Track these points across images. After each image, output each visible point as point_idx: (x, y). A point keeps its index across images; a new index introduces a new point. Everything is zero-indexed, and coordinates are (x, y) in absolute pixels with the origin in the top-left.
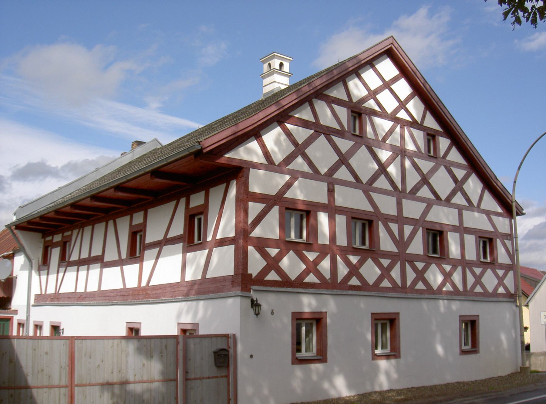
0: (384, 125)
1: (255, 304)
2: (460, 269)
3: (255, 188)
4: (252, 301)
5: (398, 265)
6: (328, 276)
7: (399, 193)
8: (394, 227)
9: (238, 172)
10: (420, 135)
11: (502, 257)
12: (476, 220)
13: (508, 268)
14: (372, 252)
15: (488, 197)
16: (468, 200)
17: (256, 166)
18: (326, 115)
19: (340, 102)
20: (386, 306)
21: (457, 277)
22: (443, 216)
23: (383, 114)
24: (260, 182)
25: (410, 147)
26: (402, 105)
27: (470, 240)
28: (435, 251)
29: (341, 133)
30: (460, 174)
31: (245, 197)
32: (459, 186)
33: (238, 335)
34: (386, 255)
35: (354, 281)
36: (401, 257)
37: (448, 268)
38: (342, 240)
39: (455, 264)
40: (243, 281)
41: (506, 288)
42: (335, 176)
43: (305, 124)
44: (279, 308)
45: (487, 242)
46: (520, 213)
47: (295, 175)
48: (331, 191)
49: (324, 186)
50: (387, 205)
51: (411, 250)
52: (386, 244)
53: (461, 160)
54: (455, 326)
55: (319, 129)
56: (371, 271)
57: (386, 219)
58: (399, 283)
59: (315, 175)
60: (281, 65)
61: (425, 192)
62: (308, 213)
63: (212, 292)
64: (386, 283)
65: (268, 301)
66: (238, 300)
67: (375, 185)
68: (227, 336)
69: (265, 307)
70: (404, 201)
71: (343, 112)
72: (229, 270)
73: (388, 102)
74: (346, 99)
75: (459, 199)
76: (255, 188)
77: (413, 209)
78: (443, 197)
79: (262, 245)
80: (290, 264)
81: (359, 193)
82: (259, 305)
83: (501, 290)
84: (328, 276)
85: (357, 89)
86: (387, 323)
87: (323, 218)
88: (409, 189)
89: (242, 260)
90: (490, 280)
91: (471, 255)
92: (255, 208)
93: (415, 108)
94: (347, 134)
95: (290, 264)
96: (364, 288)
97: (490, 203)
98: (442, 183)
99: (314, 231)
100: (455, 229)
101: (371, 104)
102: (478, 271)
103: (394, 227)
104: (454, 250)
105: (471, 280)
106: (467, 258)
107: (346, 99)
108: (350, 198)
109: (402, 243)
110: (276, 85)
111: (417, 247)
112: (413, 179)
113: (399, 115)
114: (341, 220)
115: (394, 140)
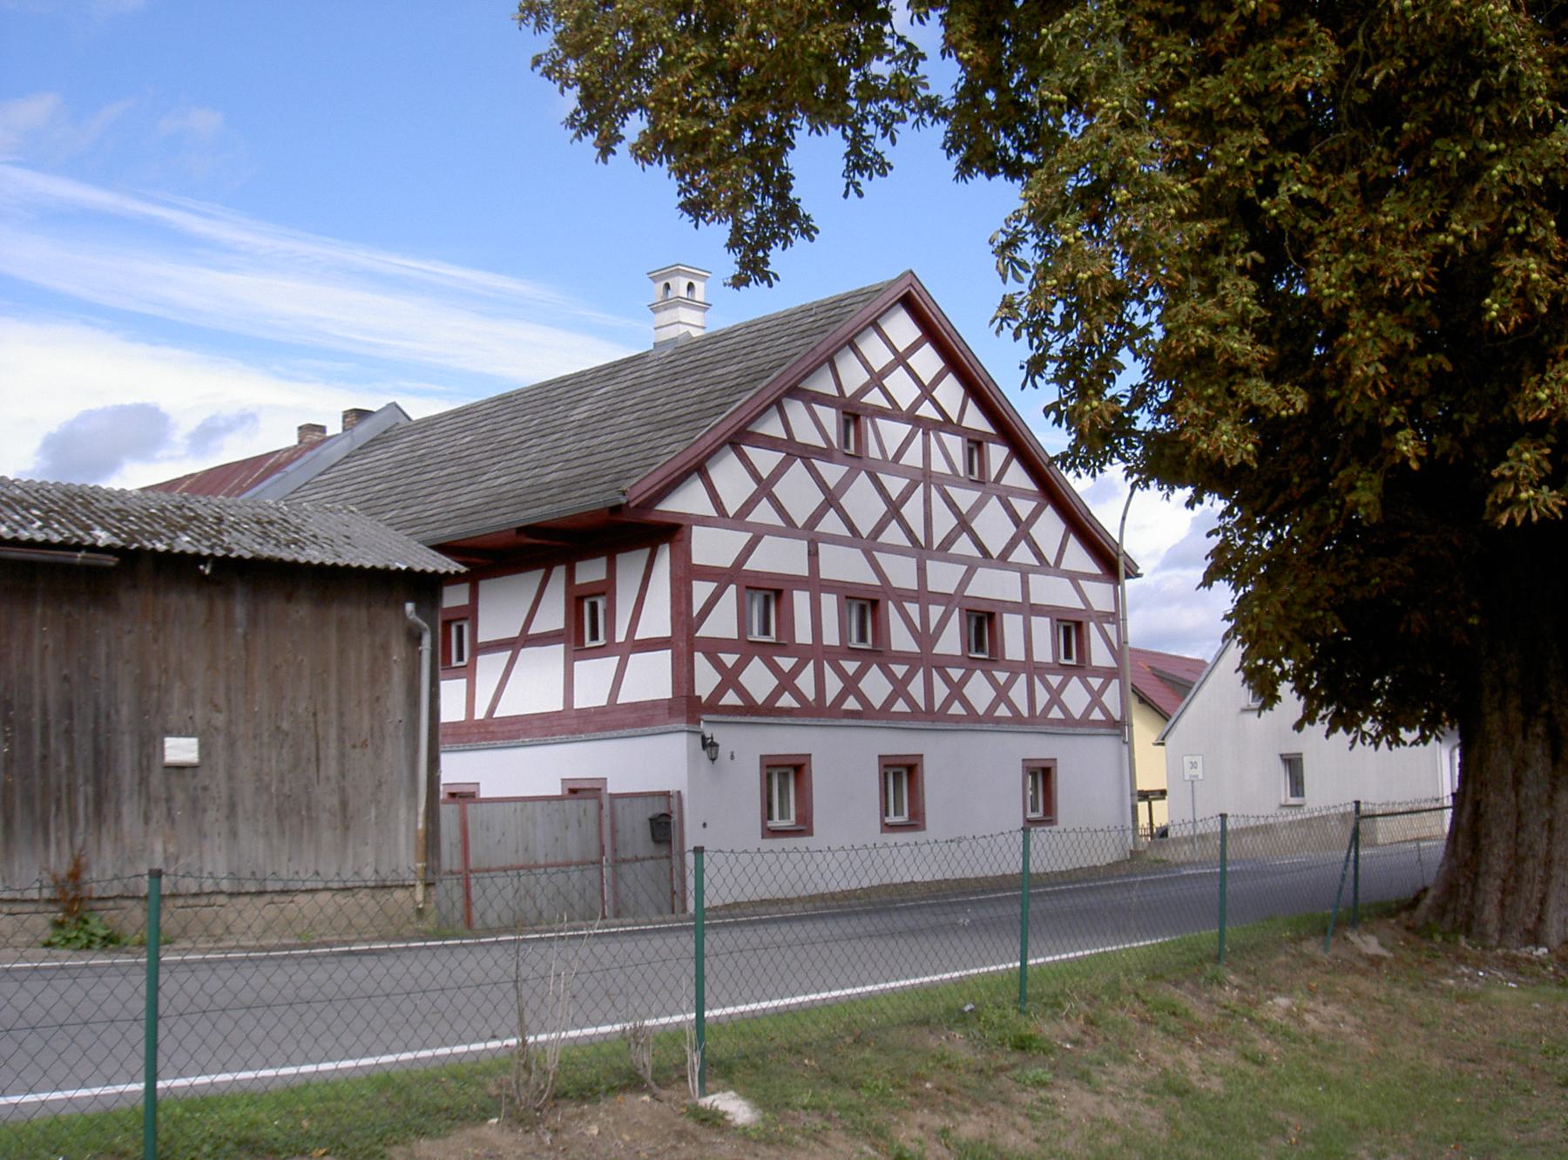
0: (893, 432)
1: (709, 745)
2: (1023, 678)
3: (698, 558)
4: (704, 738)
6: (810, 694)
7: (921, 550)
8: (913, 609)
9: (672, 532)
10: (955, 444)
11: (1100, 655)
12: (1054, 592)
13: (1109, 675)
14: (879, 654)
15: (1074, 547)
16: (1038, 554)
17: (704, 521)
18: (803, 424)
19: (824, 400)
21: (1018, 693)
22: (992, 585)
23: (894, 413)
24: (712, 547)
25: (939, 465)
26: (927, 392)
27: (1042, 628)
28: (979, 647)
29: (826, 454)
30: (1024, 508)
31: (686, 573)
32: (1023, 529)
33: (685, 793)
34: (902, 657)
35: (851, 704)
36: (926, 660)
37: (1002, 677)
38: (831, 637)
39: (1014, 669)
40: (686, 707)
41: (1104, 710)
43: (771, 443)
44: (748, 746)
45: (1071, 629)
46: (1133, 573)
48: (813, 555)
50: (901, 573)
51: (940, 649)
52: (901, 639)
53: (1029, 485)
54: (1016, 774)
55: (793, 450)
56: (876, 686)
57: (901, 596)
59: (789, 528)
60: (690, 287)
61: (964, 546)
62: (778, 593)
63: (633, 726)
64: (900, 706)
65: (725, 736)
69: (723, 752)
71: (829, 416)
72: (662, 689)
73: (903, 389)
75: (1022, 554)
76: (698, 558)
77: (943, 577)
78: (995, 554)
79: (713, 648)
80: (758, 680)
81: (857, 554)
82: (714, 745)
83: (1097, 715)
84: (810, 694)
85: (852, 375)
86: (903, 774)
87: (801, 600)
89: (683, 675)
90: (1076, 697)
91: (1044, 651)
92: (701, 591)
93: (950, 393)
94: (837, 455)
95: (758, 680)
96: (868, 715)
97: (1078, 558)
98: (994, 527)
100: (1014, 608)
101: (875, 398)
102: (1055, 680)
103: (913, 609)
104: (1013, 649)
105: (1042, 697)
106: (1036, 658)
109: (926, 638)
110: (683, 329)
111: (951, 642)
112: (944, 522)
114: (829, 602)
115: (913, 457)
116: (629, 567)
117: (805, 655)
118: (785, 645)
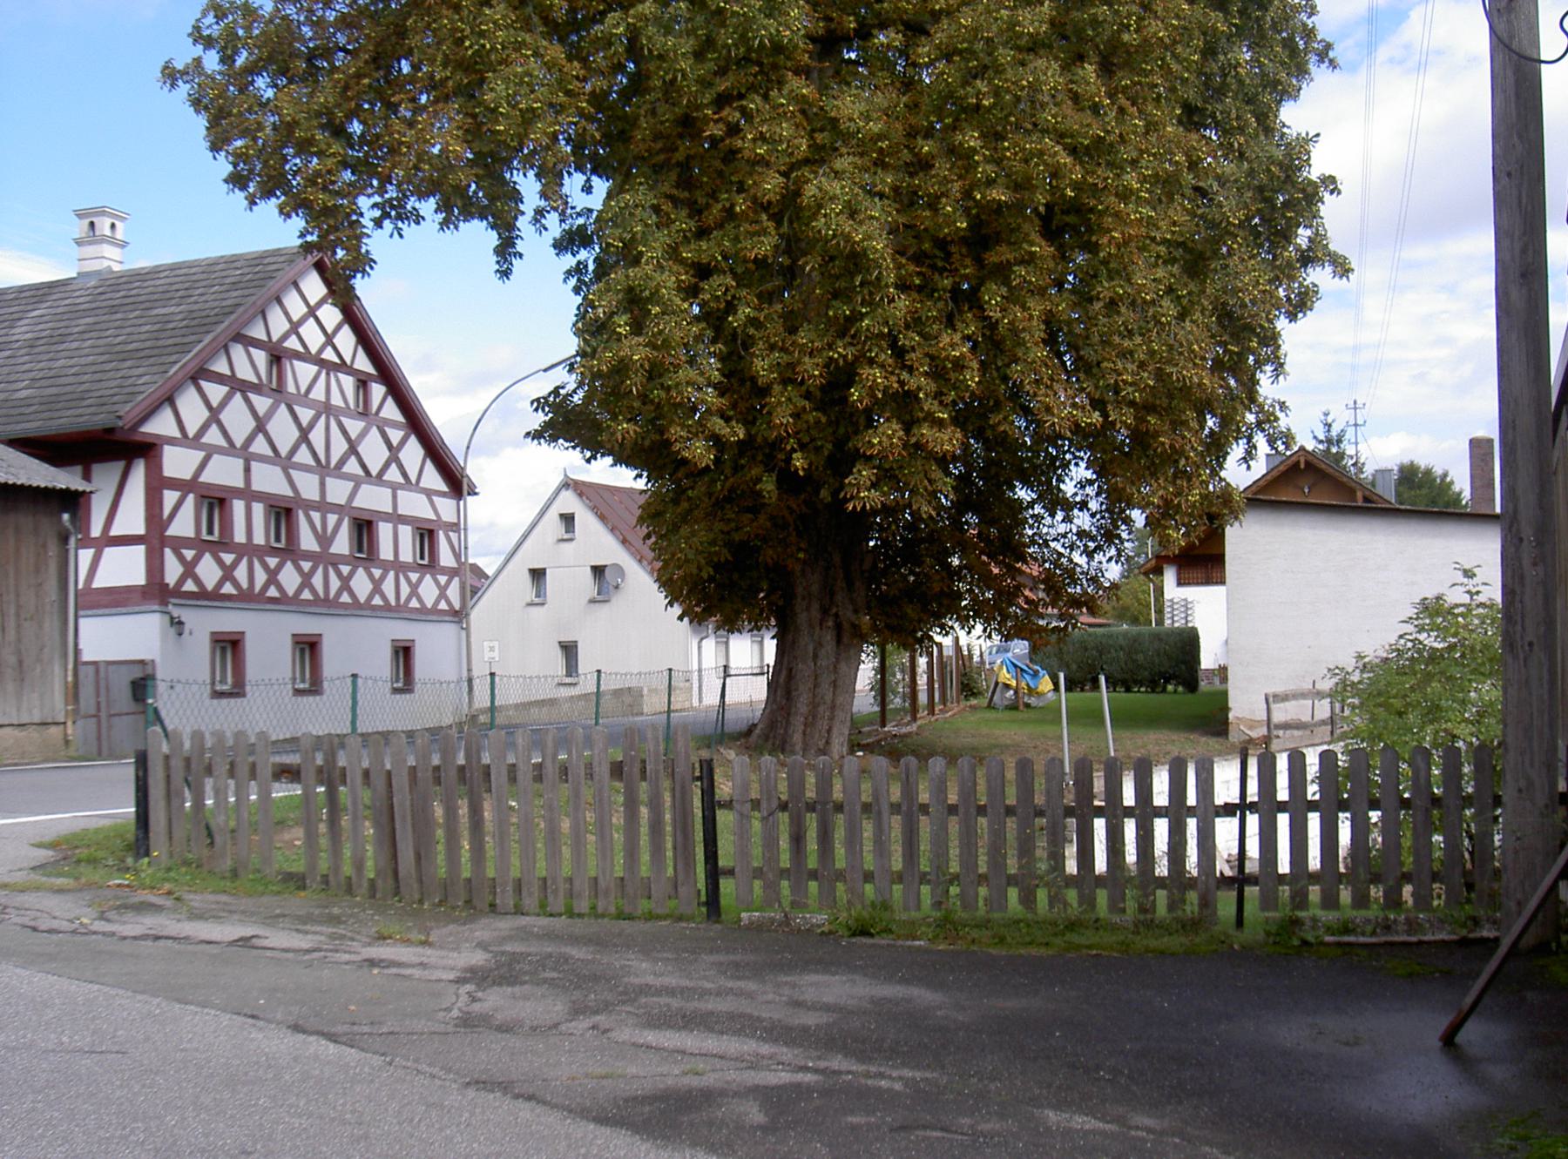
0: (306, 371)
1: (177, 624)
2: (392, 574)
3: (168, 472)
4: (172, 618)
5: (320, 570)
6: (245, 585)
7: (323, 469)
8: (316, 516)
9: (148, 450)
10: (348, 382)
11: (446, 558)
12: (415, 505)
13: (452, 573)
14: (290, 551)
15: (430, 470)
16: (405, 475)
17: (172, 441)
18: (247, 364)
19: (256, 343)
20: (307, 625)
21: (388, 586)
22: (373, 499)
23: (306, 357)
24: (178, 462)
25: (336, 400)
26: (329, 340)
27: (406, 532)
28: (360, 551)
29: (257, 388)
30: (395, 436)
31: (156, 485)
32: (394, 450)
33: (158, 660)
34: (308, 556)
35: (273, 592)
36: (325, 559)
37: (377, 573)
38: (259, 539)
39: (386, 566)
40: (156, 592)
41: (449, 603)
42: (251, 449)
43: (219, 379)
44: (204, 623)
45: (427, 535)
46: (473, 493)
47: (211, 451)
48: (247, 470)
49: (239, 463)
50: (308, 487)
52: (308, 542)
53: (400, 418)
54: (387, 653)
55: (237, 386)
56: (290, 578)
57: (309, 506)
58: (321, 594)
59: (231, 449)
60: (113, 226)
61: (352, 466)
62: (222, 501)
63: (106, 607)
64: (306, 595)
65: (187, 616)
66: (157, 616)
67: (295, 459)
68: (142, 662)
69: (187, 628)
70: (328, 480)
71: (260, 357)
72: (139, 578)
73: (312, 335)
74: (265, 338)
75: (393, 474)
76: (168, 472)
77: (338, 491)
78: (374, 473)
79: (178, 544)
80: (208, 571)
81: (278, 470)
82: (181, 623)
83: (443, 606)
84: (245, 585)
85: (278, 325)
86: (308, 647)
87: (238, 506)
88: (333, 463)
89: (154, 566)
90: (428, 590)
91: (407, 555)
92: (170, 497)
93: (346, 340)
94: (266, 390)
95: (208, 571)
96: (285, 602)
97: (433, 479)
98: (374, 451)
99: (227, 526)
100: (387, 517)
101: (292, 343)
102: (414, 577)
103: (316, 516)
104: (386, 552)
105: (405, 590)
106: (402, 559)
107: (265, 338)
108: (269, 480)
109: (325, 540)
110: (106, 263)
111: (342, 544)
112: (339, 447)
113: (324, 356)
114: (258, 509)
115: (318, 394)
116: (104, 479)
117: (386, 566)
118: (225, 543)
